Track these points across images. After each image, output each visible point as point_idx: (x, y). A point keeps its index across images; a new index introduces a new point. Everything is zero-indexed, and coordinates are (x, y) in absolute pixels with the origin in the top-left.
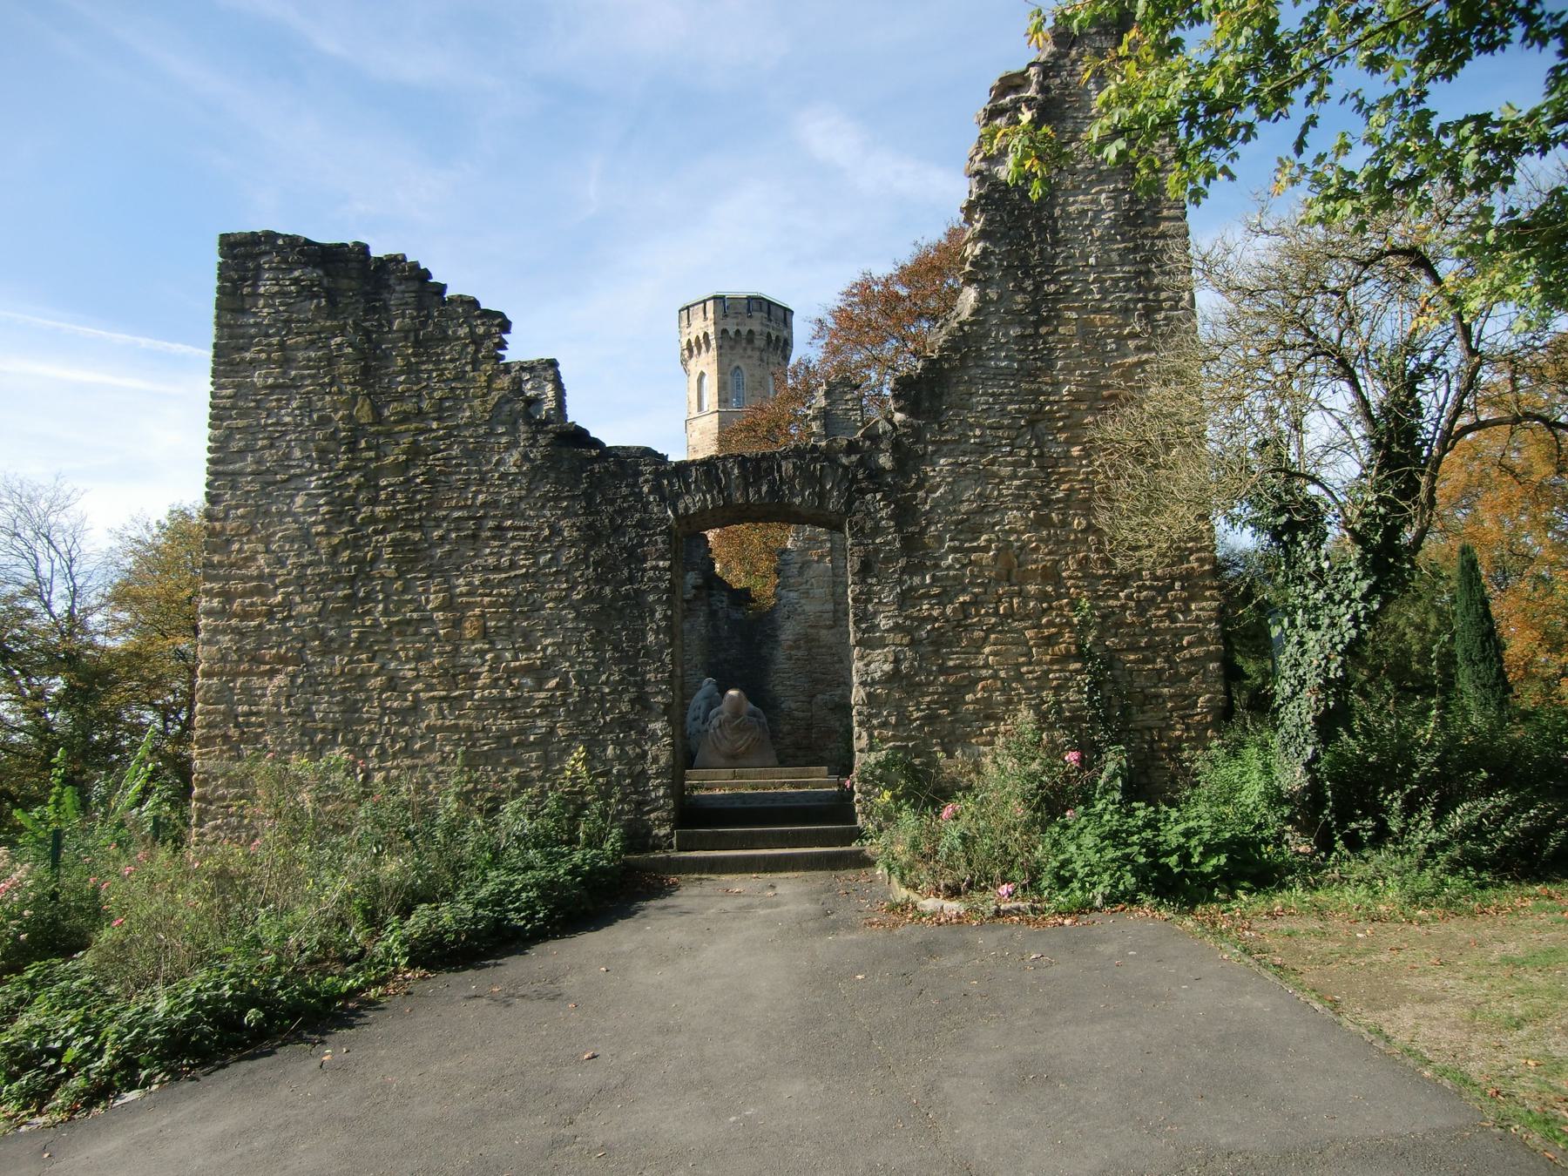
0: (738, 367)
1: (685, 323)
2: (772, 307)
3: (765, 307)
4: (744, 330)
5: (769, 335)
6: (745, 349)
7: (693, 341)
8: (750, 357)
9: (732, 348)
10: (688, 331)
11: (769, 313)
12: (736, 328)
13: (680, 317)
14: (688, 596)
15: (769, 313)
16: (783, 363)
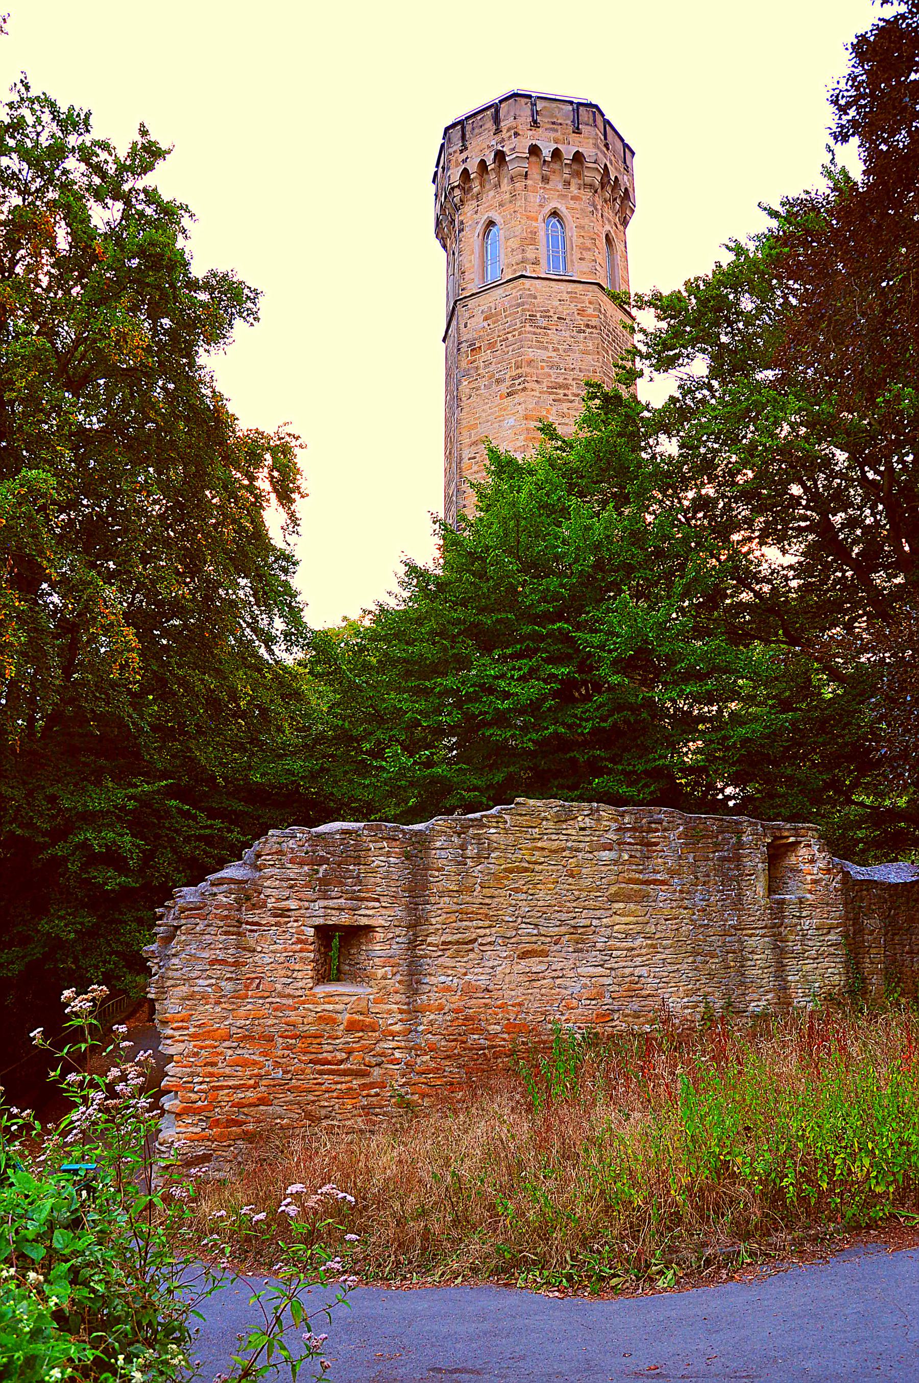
0: (555, 214)
4: (568, 152)
6: (567, 183)
9: (545, 179)
16: (621, 227)
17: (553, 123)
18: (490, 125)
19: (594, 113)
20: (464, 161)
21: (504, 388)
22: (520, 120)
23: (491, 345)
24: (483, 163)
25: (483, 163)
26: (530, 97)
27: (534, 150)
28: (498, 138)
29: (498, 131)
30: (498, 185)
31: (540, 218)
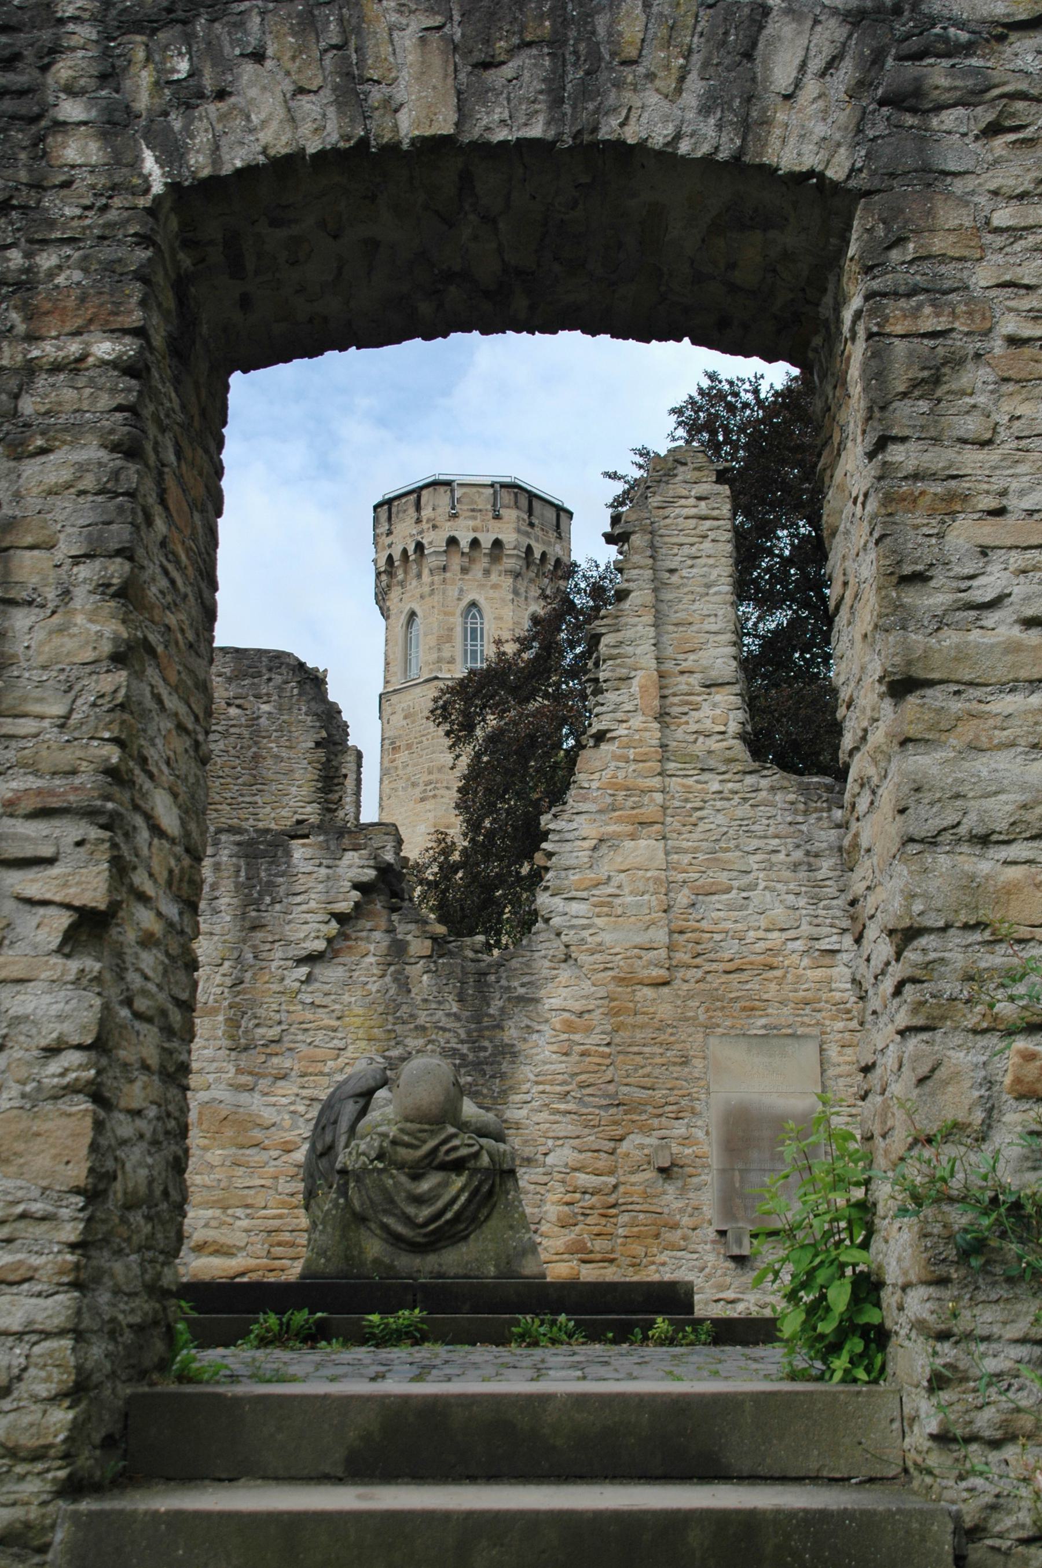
0: (473, 604)
1: (384, 528)
2: (536, 504)
3: (523, 501)
4: (486, 541)
5: (529, 550)
7: (397, 556)
8: (495, 587)
9: (464, 570)
10: (388, 540)
11: (530, 512)
12: (471, 535)
13: (376, 520)
14: (345, 906)
15: (530, 512)
17: (473, 510)
18: (412, 511)
19: (516, 494)
20: (390, 546)
21: (417, 792)
22: (440, 511)
23: (409, 746)
24: (405, 551)
25: (405, 551)
26: (448, 484)
27: (452, 541)
28: (419, 527)
29: (418, 521)
30: (419, 576)
31: (458, 612)
